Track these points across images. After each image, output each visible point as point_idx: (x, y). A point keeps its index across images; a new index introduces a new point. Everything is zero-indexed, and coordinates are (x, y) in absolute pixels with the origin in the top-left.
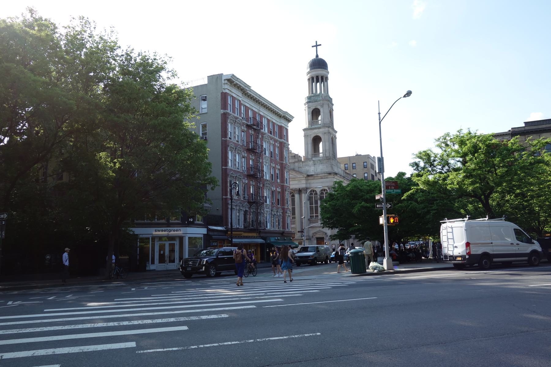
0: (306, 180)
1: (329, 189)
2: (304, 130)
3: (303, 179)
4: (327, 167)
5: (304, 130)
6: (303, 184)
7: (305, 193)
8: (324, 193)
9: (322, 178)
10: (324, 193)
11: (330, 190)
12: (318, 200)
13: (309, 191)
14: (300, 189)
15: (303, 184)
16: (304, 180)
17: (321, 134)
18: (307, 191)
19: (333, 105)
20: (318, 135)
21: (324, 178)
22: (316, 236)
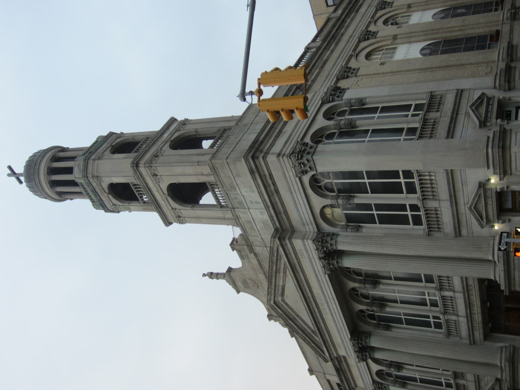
0: (290, 239)
1: (306, 172)
2: (168, 223)
3: (289, 245)
4: (239, 176)
5: (168, 223)
6: (305, 245)
7: (333, 242)
8: (326, 181)
9: (277, 191)
10: (326, 181)
11: (309, 169)
12: (351, 202)
13: (326, 228)
14: (322, 256)
15: (305, 245)
16: (291, 244)
17: (160, 184)
18: (328, 234)
19: (111, 134)
20: (166, 192)
21: (274, 184)
22: (491, 217)
